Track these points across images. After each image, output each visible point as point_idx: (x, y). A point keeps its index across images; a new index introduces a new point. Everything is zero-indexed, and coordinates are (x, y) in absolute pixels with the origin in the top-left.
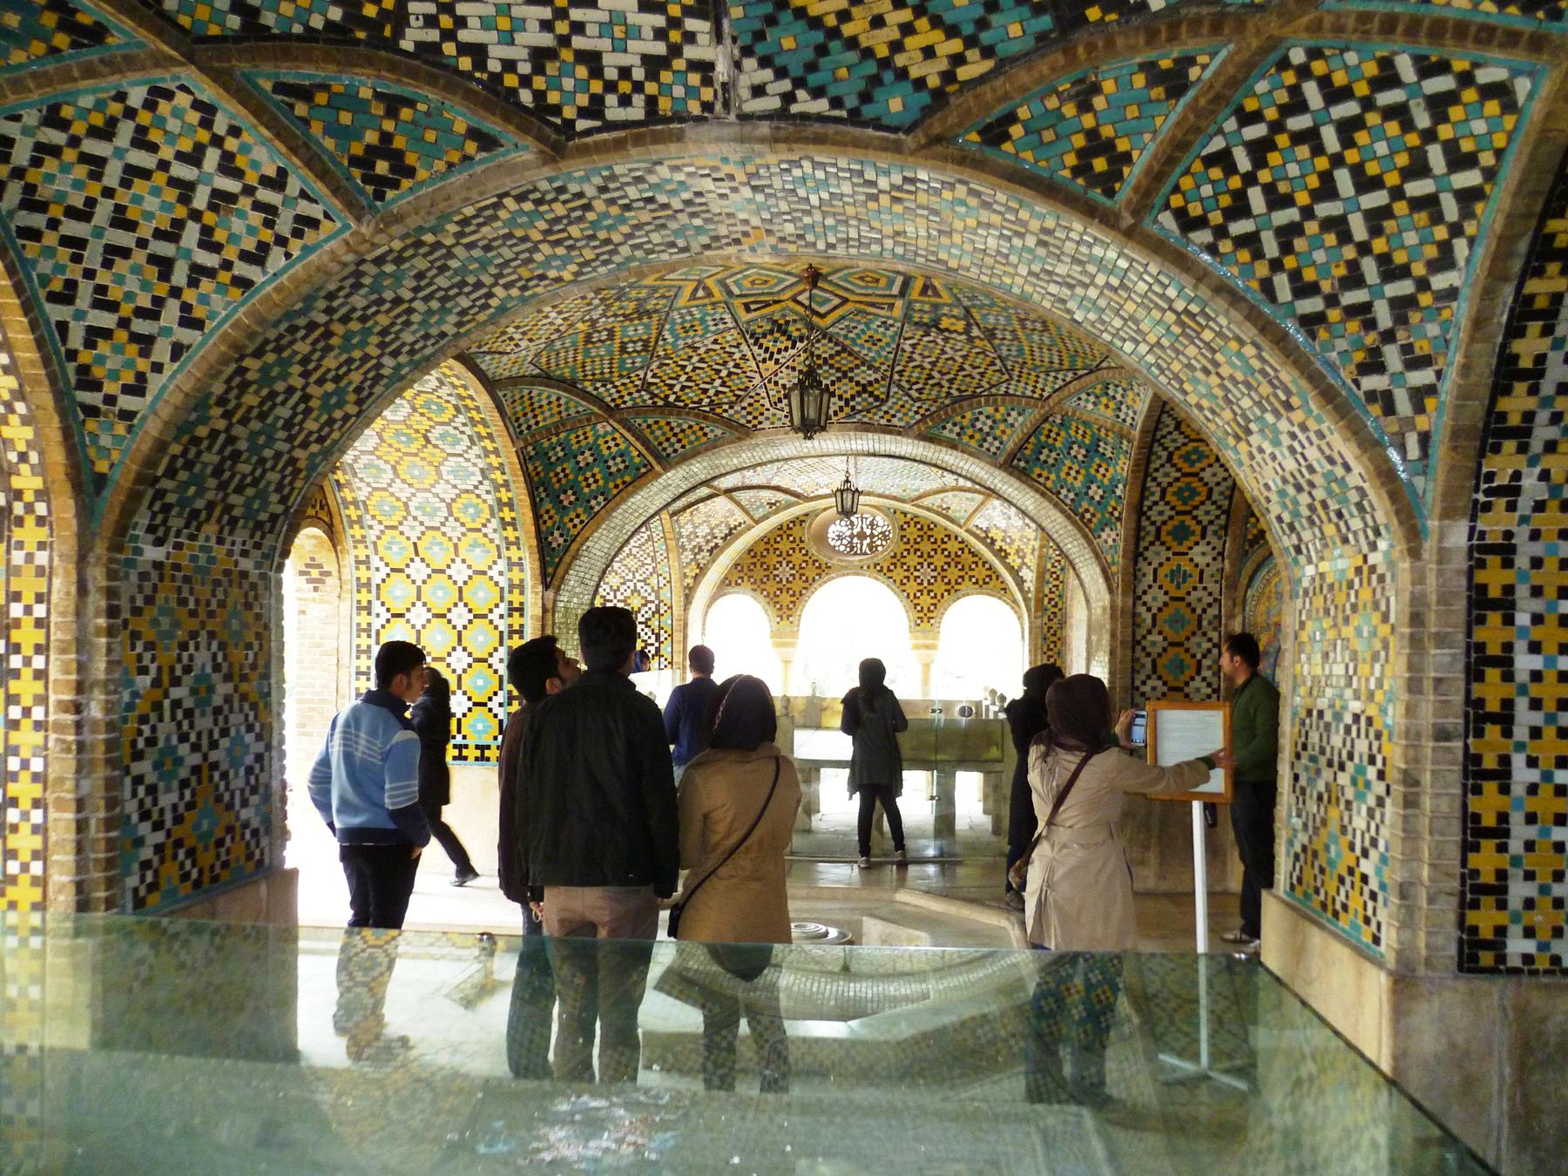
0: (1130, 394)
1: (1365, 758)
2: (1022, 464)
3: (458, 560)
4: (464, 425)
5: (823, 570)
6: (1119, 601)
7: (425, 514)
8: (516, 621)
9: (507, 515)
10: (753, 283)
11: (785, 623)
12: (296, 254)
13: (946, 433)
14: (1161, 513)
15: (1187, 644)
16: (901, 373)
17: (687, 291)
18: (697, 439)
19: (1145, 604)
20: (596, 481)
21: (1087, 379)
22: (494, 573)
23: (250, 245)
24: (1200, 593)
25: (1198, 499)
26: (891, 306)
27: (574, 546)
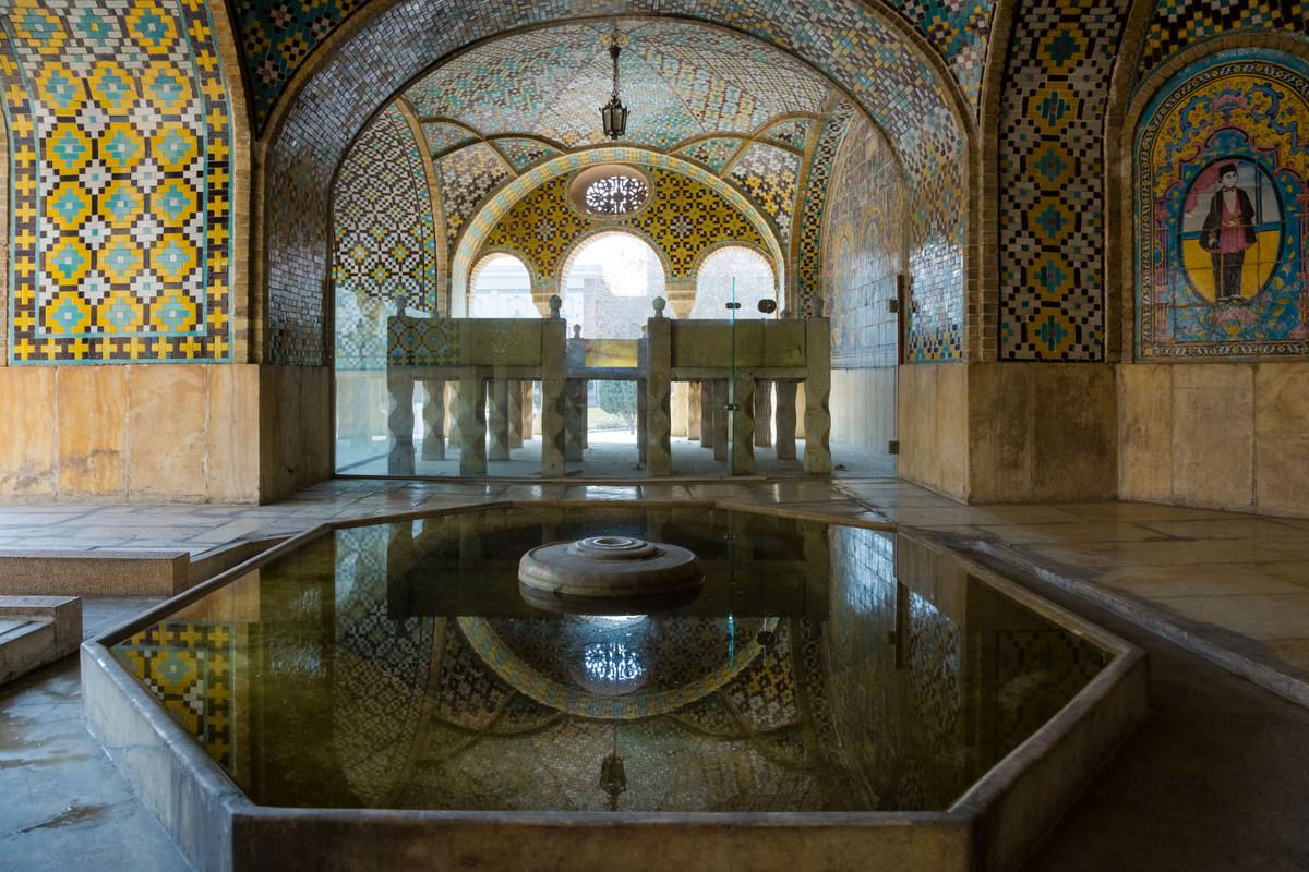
3: (143, 102)
6: (980, 142)
9: (200, 32)
11: (546, 277)
14: (1042, 18)
15: (1063, 194)
19: (1011, 143)
24: (1078, 131)
27: (293, 86)
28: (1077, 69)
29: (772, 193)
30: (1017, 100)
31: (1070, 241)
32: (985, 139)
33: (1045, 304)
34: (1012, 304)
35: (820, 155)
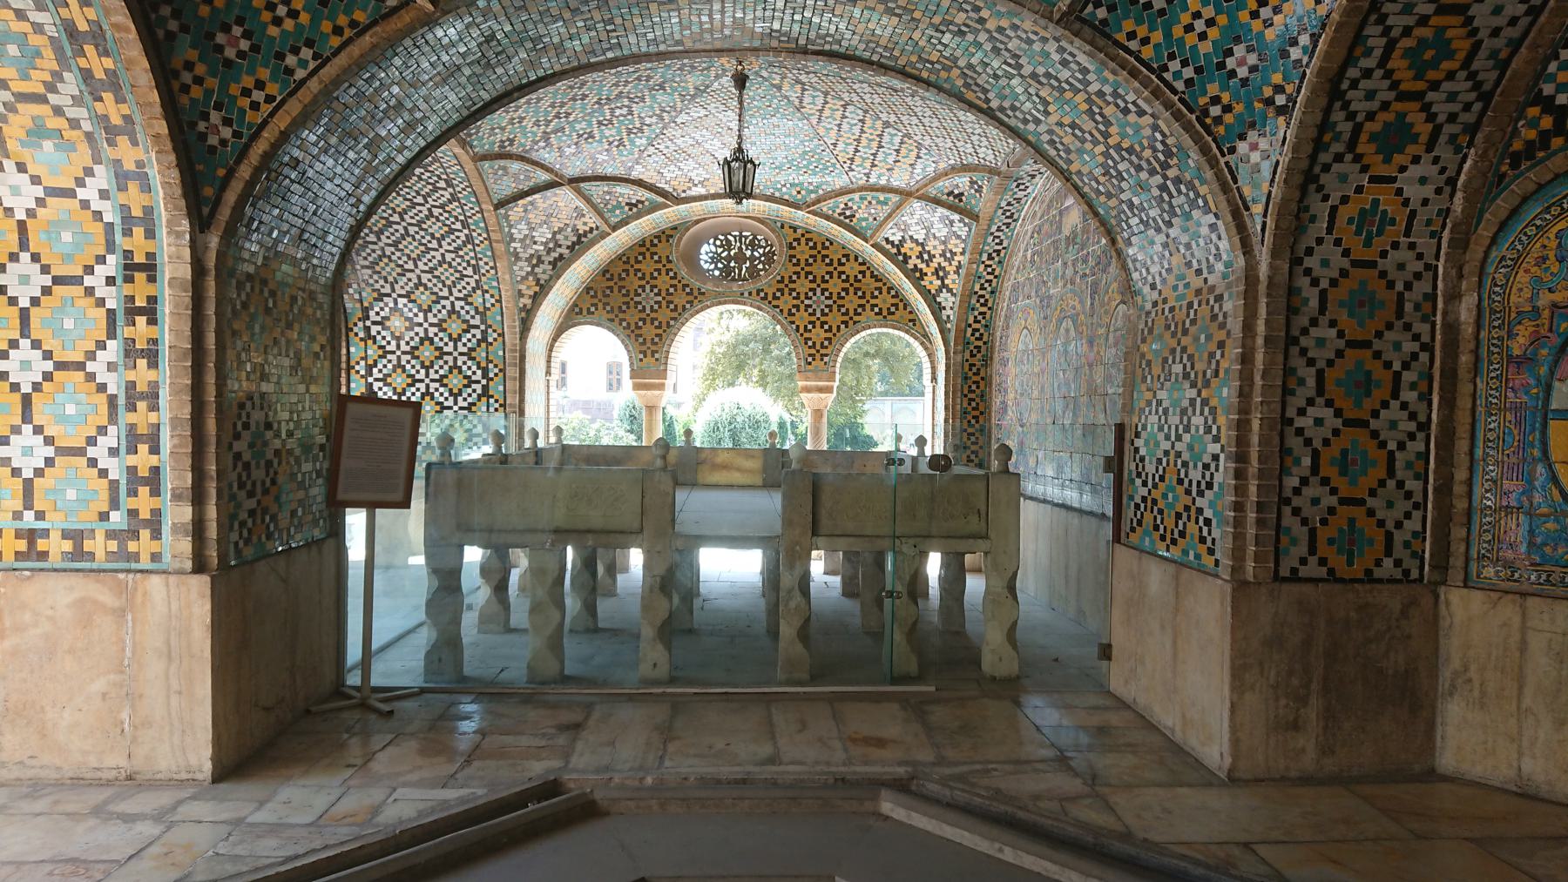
5: (696, 300)
6: (1263, 270)
8: (141, 290)
11: (649, 360)
14: (1370, 95)
19: (1308, 272)
22: (88, 193)
24: (1404, 255)
25: (1446, 65)
27: (260, 147)
28: (1412, 168)
29: (934, 265)
30: (1322, 210)
31: (1383, 412)
32: (1271, 266)
33: (1342, 501)
34: (1296, 501)
35: (1000, 219)
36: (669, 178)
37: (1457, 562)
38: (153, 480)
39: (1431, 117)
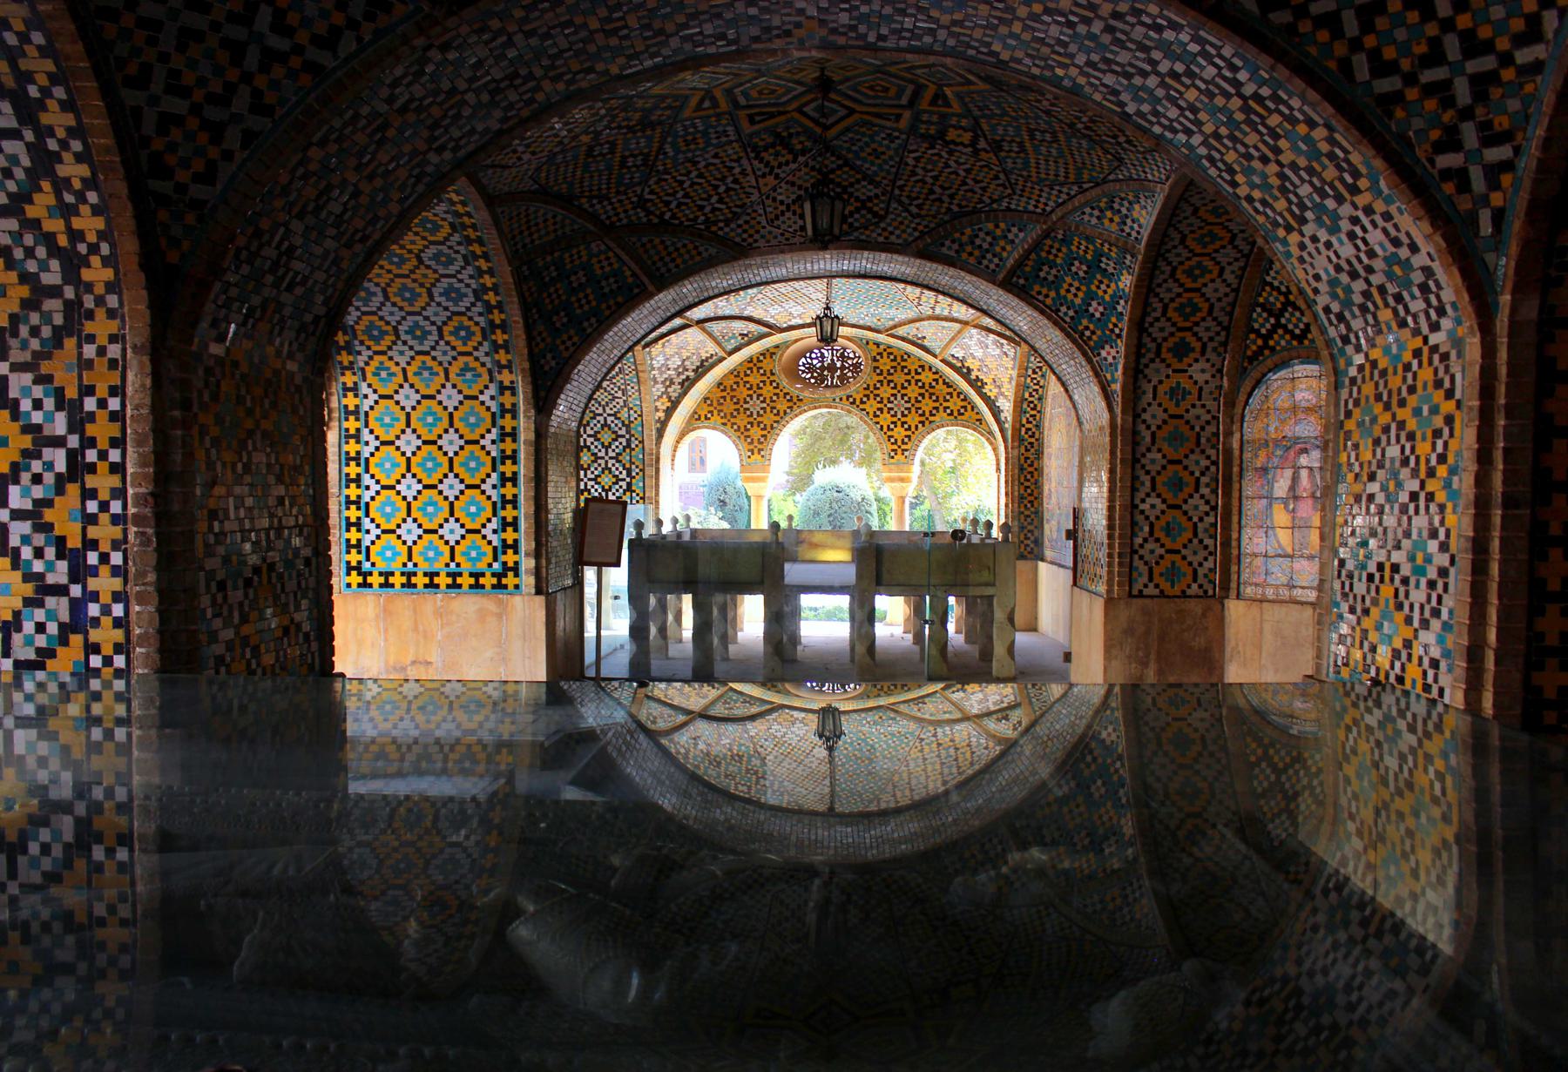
0: (1137, 207)
1: (1425, 534)
2: (1022, 281)
3: (449, 385)
4: (459, 244)
5: (795, 405)
7: (415, 338)
8: (509, 446)
9: (500, 337)
10: (760, 93)
11: (756, 456)
12: (367, 38)
13: (944, 250)
14: (1162, 330)
16: (901, 188)
17: (693, 102)
18: (692, 258)
19: (1144, 421)
20: (589, 302)
21: (1094, 193)
23: (321, 28)
24: (1199, 411)
26: (898, 117)
30: (1149, 389)
33: (1168, 551)
36: (774, 314)
37: (1233, 585)
38: (515, 547)
39: (1199, 339)
